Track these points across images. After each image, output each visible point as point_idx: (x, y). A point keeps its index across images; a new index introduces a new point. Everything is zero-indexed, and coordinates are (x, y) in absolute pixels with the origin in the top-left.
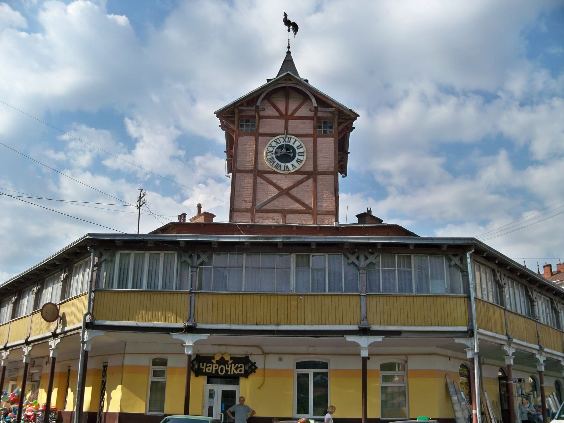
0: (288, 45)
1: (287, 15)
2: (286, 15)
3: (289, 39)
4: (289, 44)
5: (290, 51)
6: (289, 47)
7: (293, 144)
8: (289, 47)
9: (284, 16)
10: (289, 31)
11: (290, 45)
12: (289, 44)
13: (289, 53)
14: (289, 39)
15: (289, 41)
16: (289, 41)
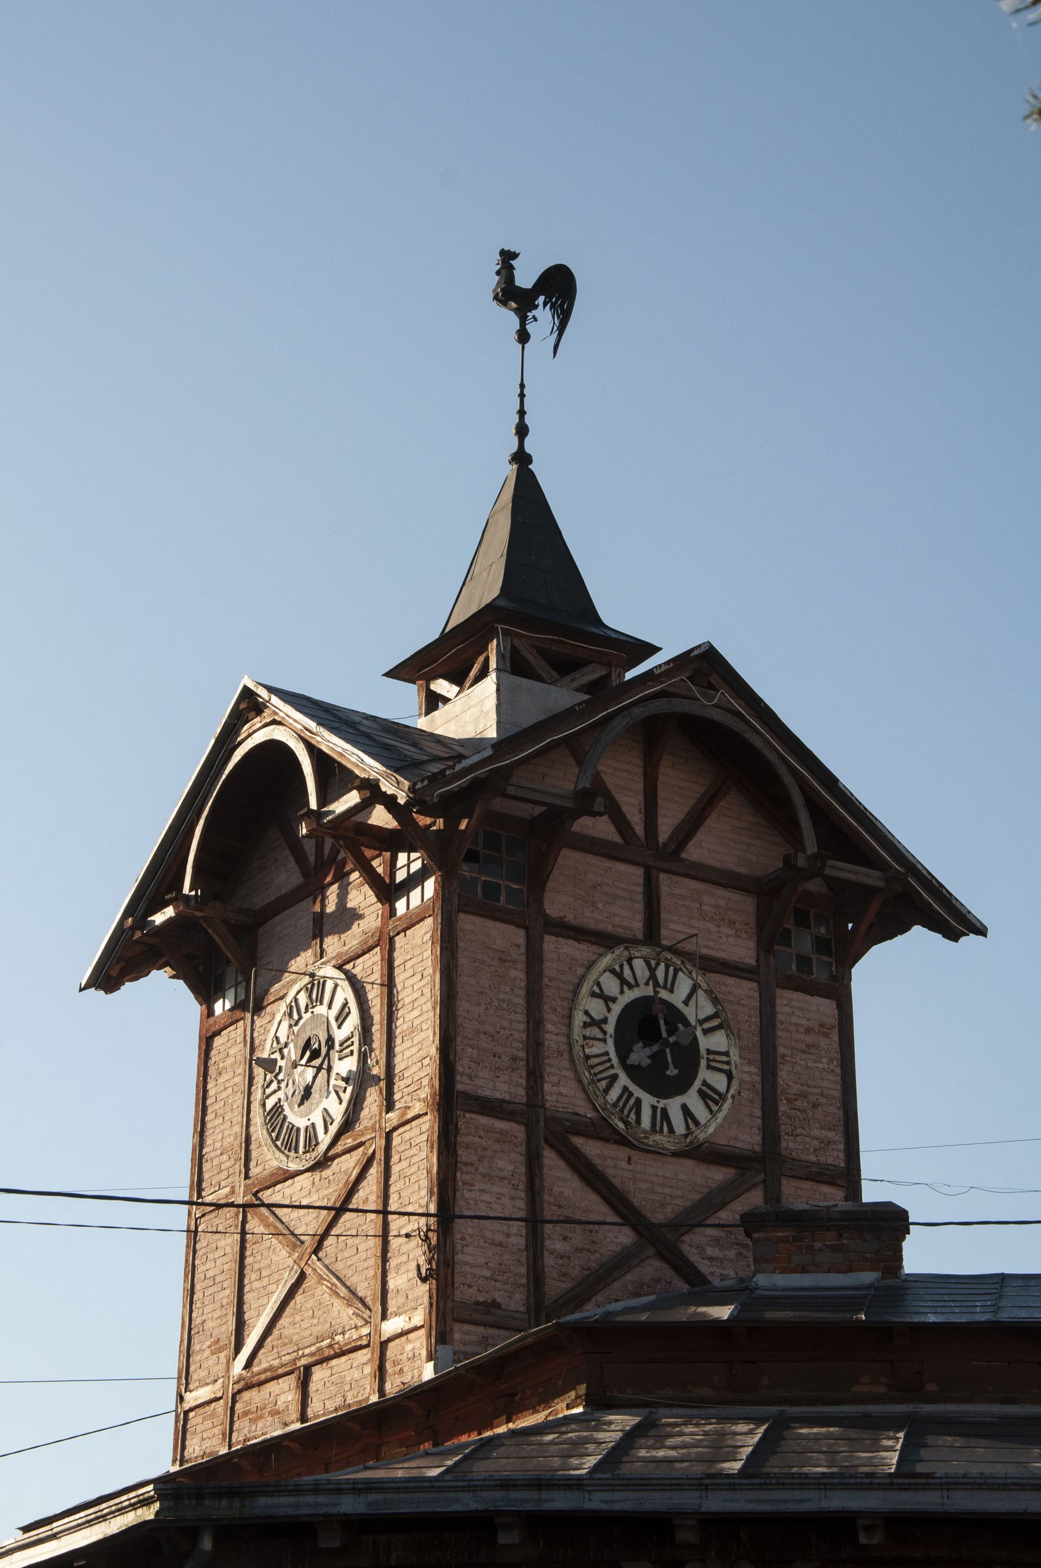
0: (516, 419)
1: (514, 255)
2: (508, 257)
3: (522, 386)
4: (522, 413)
5: (528, 449)
6: (522, 431)
7: (330, 1007)
8: (522, 431)
9: (498, 273)
10: (523, 337)
11: (528, 420)
12: (522, 413)
13: (522, 458)
14: (522, 386)
15: (522, 396)
16: (522, 396)
